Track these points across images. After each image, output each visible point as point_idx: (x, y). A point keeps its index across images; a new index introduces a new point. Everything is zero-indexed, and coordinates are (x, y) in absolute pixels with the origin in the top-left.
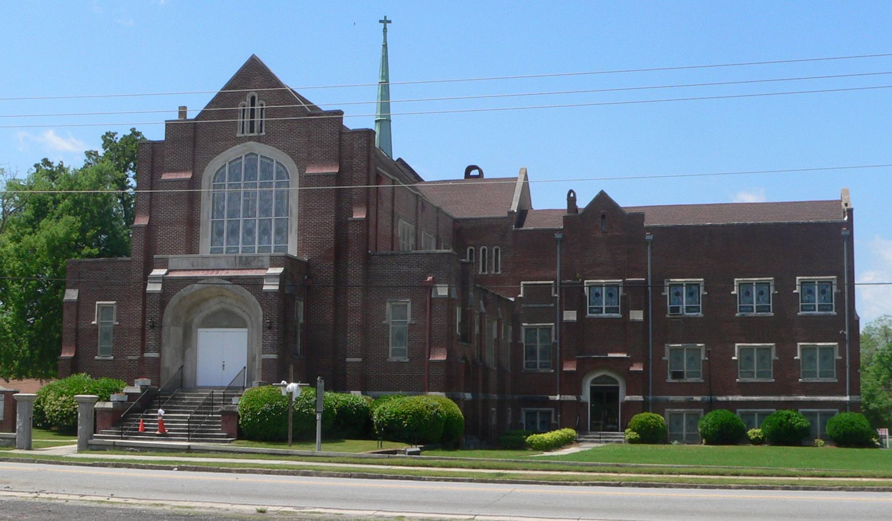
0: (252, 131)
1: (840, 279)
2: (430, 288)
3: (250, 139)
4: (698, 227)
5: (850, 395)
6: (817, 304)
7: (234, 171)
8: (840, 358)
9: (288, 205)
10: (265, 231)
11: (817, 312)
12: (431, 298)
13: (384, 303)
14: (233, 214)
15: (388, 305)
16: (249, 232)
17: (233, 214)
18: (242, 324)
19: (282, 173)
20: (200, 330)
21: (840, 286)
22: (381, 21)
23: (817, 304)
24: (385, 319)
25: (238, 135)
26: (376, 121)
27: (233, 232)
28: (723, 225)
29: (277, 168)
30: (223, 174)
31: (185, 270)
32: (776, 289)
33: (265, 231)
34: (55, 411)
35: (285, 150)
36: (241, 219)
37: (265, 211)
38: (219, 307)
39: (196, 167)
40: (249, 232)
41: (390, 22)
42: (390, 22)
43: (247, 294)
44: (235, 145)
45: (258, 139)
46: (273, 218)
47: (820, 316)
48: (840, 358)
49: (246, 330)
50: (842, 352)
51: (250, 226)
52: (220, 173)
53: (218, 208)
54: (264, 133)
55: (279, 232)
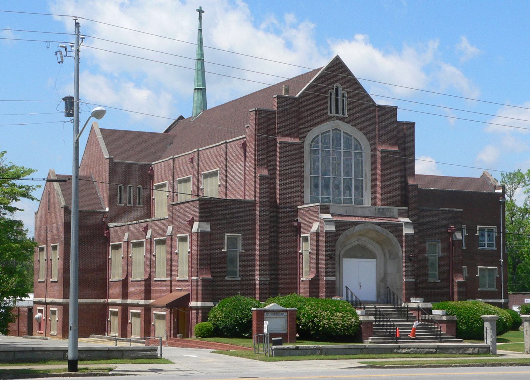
0: (337, 112)
1: (499, 228)
2: (451, 234)
3: (338, 118)
4: (427, 190)
5: (504, 298)
6: (486, 242)
7: (325, 140)
8: (498, 276)
9: (362, 170)
11: (486, 248)
12: (453, 241)
13: (425, 243)
15: (427, 244)
16: (337, 187)
19: (358, 146)
20: (344, 259)
21: (499, 232)
22: (198, 10)
23: (486, 242)
24: (425, 253)
25: (329, 114)
26: (195, 89)
28: (440, 190)
29: (354, 142)
32: (467, 233)
33: (348, 188)
35: (362, 130)
36: (332, 177)
37: (348, 173)
38: (357, 243)
39: (300, 134)
40: (337, 187)
41: (203, 12)
42: (203, 12)
43: (391, 236)
44: (327, 121)
45: (343, 119)
47: (489, 250)
48: (498, 276)
50: (500, 273)
51: (337, 182)
52: (315, 140)
53: (314, 167)
54: (346, 116)
55: (357, 188)
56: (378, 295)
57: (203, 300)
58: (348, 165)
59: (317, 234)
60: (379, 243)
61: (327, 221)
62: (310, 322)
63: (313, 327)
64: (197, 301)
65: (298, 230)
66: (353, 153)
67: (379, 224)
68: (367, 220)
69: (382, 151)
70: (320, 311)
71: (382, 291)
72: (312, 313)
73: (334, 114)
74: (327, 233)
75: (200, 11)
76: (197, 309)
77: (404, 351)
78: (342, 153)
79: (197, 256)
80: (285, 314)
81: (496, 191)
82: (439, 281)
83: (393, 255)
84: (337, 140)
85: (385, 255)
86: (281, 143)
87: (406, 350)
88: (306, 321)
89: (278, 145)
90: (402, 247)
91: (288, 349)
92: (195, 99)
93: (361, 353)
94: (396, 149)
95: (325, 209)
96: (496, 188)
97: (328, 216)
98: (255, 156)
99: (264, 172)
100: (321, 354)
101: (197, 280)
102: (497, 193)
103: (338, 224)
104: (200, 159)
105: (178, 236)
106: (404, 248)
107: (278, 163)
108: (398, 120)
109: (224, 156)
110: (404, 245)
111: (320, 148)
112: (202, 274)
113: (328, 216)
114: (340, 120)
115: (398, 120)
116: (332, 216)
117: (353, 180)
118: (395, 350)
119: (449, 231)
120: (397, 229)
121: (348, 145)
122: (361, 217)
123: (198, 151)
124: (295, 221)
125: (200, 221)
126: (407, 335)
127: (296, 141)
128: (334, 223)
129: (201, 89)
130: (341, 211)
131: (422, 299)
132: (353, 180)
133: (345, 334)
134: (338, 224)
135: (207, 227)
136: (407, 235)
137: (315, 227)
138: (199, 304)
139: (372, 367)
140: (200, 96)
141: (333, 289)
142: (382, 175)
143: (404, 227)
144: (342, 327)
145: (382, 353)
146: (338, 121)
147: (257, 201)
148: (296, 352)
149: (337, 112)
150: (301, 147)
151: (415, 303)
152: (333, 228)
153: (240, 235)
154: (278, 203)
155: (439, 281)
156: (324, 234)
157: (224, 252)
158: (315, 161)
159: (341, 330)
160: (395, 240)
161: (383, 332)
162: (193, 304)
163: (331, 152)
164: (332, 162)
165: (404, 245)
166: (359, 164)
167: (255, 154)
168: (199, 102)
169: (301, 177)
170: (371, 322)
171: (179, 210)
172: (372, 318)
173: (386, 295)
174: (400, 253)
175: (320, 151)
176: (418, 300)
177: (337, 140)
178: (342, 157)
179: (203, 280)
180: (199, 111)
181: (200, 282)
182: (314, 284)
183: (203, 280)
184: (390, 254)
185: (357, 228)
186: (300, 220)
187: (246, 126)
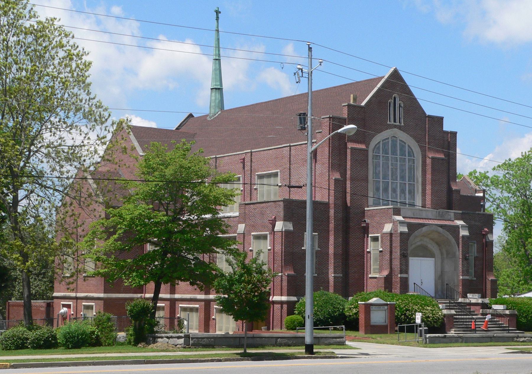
0: (395, 121)
3: (395, 127)
10: (403, 191)
12: (486, 242)
14: (385, 177)
16: (394, 191)
17: (385, 177)
18: (431, 255)
19: (411, 153)
26: (212, 89)
27: (386, 190)
30: (379, 147)
31: (410, 218)
33: (403, 191)
34: (429, 317)
37: (403, 178)
40: (394, 191)
41: (220, 12)
42: (220, 12)
43: (450, 237)
44: (387, 129)
45: (400, 128)
46: (407, 183)
49: (434, 259)
51: (394, 186)
52: (377, 147)
53: (376, 173)
54: (403, 124)
55: (410, 192)
56: (436, 292)
57: (288, 295)
58: (403, 171)
59: (391, 234)
60: (438, 244)
61: (401, 223)
62: (402, 315)
63: (405, 320)
64: (281, 296)
65: (366, 230)
66: (407, 160)
67: (441, 226)
68: (431, 222)
69: (433, 159)
70: (411, 305)
71: (439, 287)
72: (405, 307)
73: (392, 123)
74: (402, 233)
75: (218, 12)
76: (281, 303)
77: (522, 340)
78: (398, 159)
79: (282, 253)
80: (386, 307)
81: (477, 195)
82: (475, 279)
83: (451, 255)
84: (394, 146)
85: (442, 254)
86: (352, 149)
87: (523, 339)
88: (398, 314)
89: (349, 151)
90: (459, 247)
91: (439, 337)
92: (213, 98)
93: (491, 341)
94: (442, 156)
95: (397, 212)
96: (476, 191)
97: (400, 218)
98: (329, 161)
99: (337, 176)
100: (462, 342)
101: (282, 276)
102: (478, 197)
103: (409, 225)
104: (253, 160)
105: (252, 234)
106: (461, 248)
107: (348, 167)
108: (444, 129)
109: (287, 159)
110: (460, 246)
111: (381, 154)
112: (286, 270)
113: (400, 218)
114: (397, 128)
115: (444, 129)
116: (404, 217)
117: (407, 184)
118: (515, 339)
119: (483, 233)
120: (455, 230)
121: (403, 153)
122: (425, 219)
123: (251, 152)
124: (363, 222)
125: (285, 220)
126: (480, 328)
127: (363, 147)
128: (406, 225)
129: (219, 89)
130: (409, 214)
131: (480, 295)
132: (407, 184)
133: (434, 326)
134: (409, 225)
135: (290, 227)
136: (463, 237)
137: (388, 228)
138: (284, 298)
139: (522, 352)
140: (218, 96)
141: (405, 285)
142: (433, 181)
143: (460, 229)
144: (432, 320)
145: (505, 342)
146: (396, 129)
147: (332, 201)
148: (444, 340)
149: (395, 121)
150: (366, 151)
151: (474, 298)
152: (405, 229)
153: (317, 234)
154: (349, 205)
155: (475, 279)
156: (399, 235)
157: (303, 250)
158: (376, 166)
159: (431, 322)
160: (453, 241)
161: (460, 325)
162: (276, 298)
163: (390, 158)
164: (390, 167)
165: (460, 246)
166: (412, 169)
167: (329, 159)
168: (217, 101)
169: (366, 180)
170: (452, 315)
171: (255, 209)
172: (453, 312)
173: (444, 292)
174: (458, 253)
175: (381, 157)
176: (477, 296)
177: (394, 146)
178: (399, 163)
179: (288, 276)
180: (217, 110)
181: (285, 278)
182: (388, 281)
183: (288, 276)
184: (448, 254)
185: (424, 229)
186: (368, 221)
187: (317, 131)
